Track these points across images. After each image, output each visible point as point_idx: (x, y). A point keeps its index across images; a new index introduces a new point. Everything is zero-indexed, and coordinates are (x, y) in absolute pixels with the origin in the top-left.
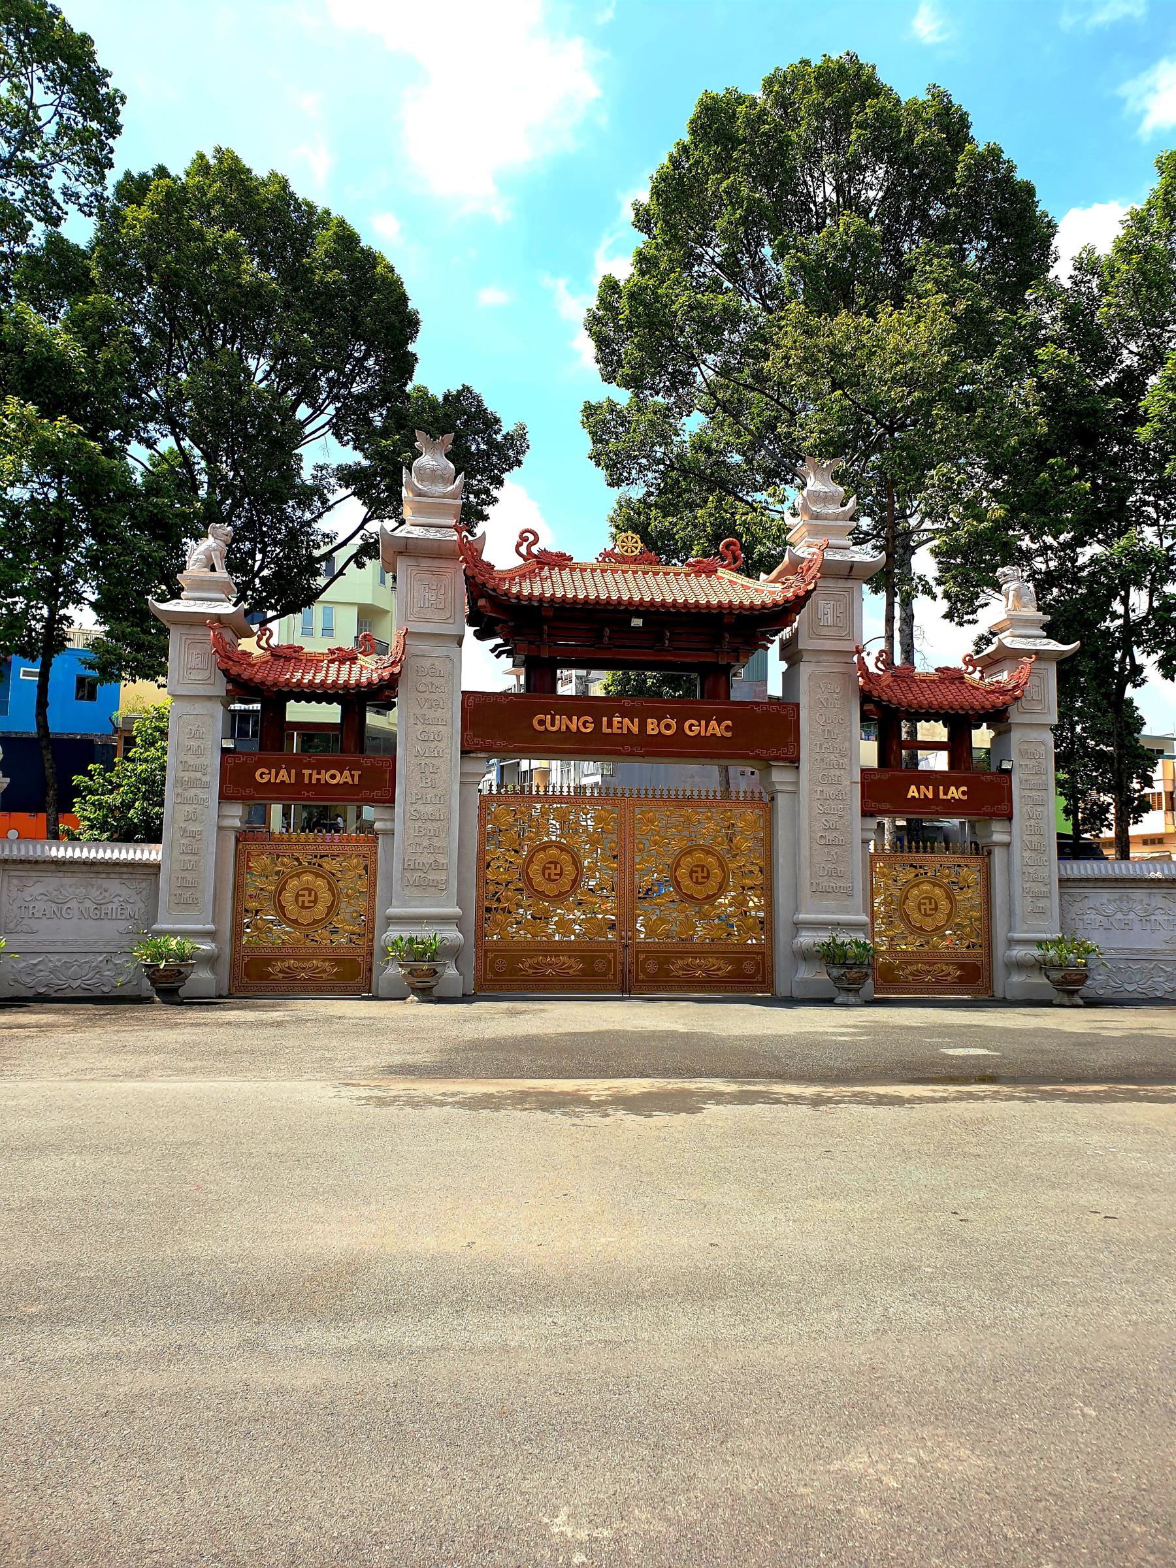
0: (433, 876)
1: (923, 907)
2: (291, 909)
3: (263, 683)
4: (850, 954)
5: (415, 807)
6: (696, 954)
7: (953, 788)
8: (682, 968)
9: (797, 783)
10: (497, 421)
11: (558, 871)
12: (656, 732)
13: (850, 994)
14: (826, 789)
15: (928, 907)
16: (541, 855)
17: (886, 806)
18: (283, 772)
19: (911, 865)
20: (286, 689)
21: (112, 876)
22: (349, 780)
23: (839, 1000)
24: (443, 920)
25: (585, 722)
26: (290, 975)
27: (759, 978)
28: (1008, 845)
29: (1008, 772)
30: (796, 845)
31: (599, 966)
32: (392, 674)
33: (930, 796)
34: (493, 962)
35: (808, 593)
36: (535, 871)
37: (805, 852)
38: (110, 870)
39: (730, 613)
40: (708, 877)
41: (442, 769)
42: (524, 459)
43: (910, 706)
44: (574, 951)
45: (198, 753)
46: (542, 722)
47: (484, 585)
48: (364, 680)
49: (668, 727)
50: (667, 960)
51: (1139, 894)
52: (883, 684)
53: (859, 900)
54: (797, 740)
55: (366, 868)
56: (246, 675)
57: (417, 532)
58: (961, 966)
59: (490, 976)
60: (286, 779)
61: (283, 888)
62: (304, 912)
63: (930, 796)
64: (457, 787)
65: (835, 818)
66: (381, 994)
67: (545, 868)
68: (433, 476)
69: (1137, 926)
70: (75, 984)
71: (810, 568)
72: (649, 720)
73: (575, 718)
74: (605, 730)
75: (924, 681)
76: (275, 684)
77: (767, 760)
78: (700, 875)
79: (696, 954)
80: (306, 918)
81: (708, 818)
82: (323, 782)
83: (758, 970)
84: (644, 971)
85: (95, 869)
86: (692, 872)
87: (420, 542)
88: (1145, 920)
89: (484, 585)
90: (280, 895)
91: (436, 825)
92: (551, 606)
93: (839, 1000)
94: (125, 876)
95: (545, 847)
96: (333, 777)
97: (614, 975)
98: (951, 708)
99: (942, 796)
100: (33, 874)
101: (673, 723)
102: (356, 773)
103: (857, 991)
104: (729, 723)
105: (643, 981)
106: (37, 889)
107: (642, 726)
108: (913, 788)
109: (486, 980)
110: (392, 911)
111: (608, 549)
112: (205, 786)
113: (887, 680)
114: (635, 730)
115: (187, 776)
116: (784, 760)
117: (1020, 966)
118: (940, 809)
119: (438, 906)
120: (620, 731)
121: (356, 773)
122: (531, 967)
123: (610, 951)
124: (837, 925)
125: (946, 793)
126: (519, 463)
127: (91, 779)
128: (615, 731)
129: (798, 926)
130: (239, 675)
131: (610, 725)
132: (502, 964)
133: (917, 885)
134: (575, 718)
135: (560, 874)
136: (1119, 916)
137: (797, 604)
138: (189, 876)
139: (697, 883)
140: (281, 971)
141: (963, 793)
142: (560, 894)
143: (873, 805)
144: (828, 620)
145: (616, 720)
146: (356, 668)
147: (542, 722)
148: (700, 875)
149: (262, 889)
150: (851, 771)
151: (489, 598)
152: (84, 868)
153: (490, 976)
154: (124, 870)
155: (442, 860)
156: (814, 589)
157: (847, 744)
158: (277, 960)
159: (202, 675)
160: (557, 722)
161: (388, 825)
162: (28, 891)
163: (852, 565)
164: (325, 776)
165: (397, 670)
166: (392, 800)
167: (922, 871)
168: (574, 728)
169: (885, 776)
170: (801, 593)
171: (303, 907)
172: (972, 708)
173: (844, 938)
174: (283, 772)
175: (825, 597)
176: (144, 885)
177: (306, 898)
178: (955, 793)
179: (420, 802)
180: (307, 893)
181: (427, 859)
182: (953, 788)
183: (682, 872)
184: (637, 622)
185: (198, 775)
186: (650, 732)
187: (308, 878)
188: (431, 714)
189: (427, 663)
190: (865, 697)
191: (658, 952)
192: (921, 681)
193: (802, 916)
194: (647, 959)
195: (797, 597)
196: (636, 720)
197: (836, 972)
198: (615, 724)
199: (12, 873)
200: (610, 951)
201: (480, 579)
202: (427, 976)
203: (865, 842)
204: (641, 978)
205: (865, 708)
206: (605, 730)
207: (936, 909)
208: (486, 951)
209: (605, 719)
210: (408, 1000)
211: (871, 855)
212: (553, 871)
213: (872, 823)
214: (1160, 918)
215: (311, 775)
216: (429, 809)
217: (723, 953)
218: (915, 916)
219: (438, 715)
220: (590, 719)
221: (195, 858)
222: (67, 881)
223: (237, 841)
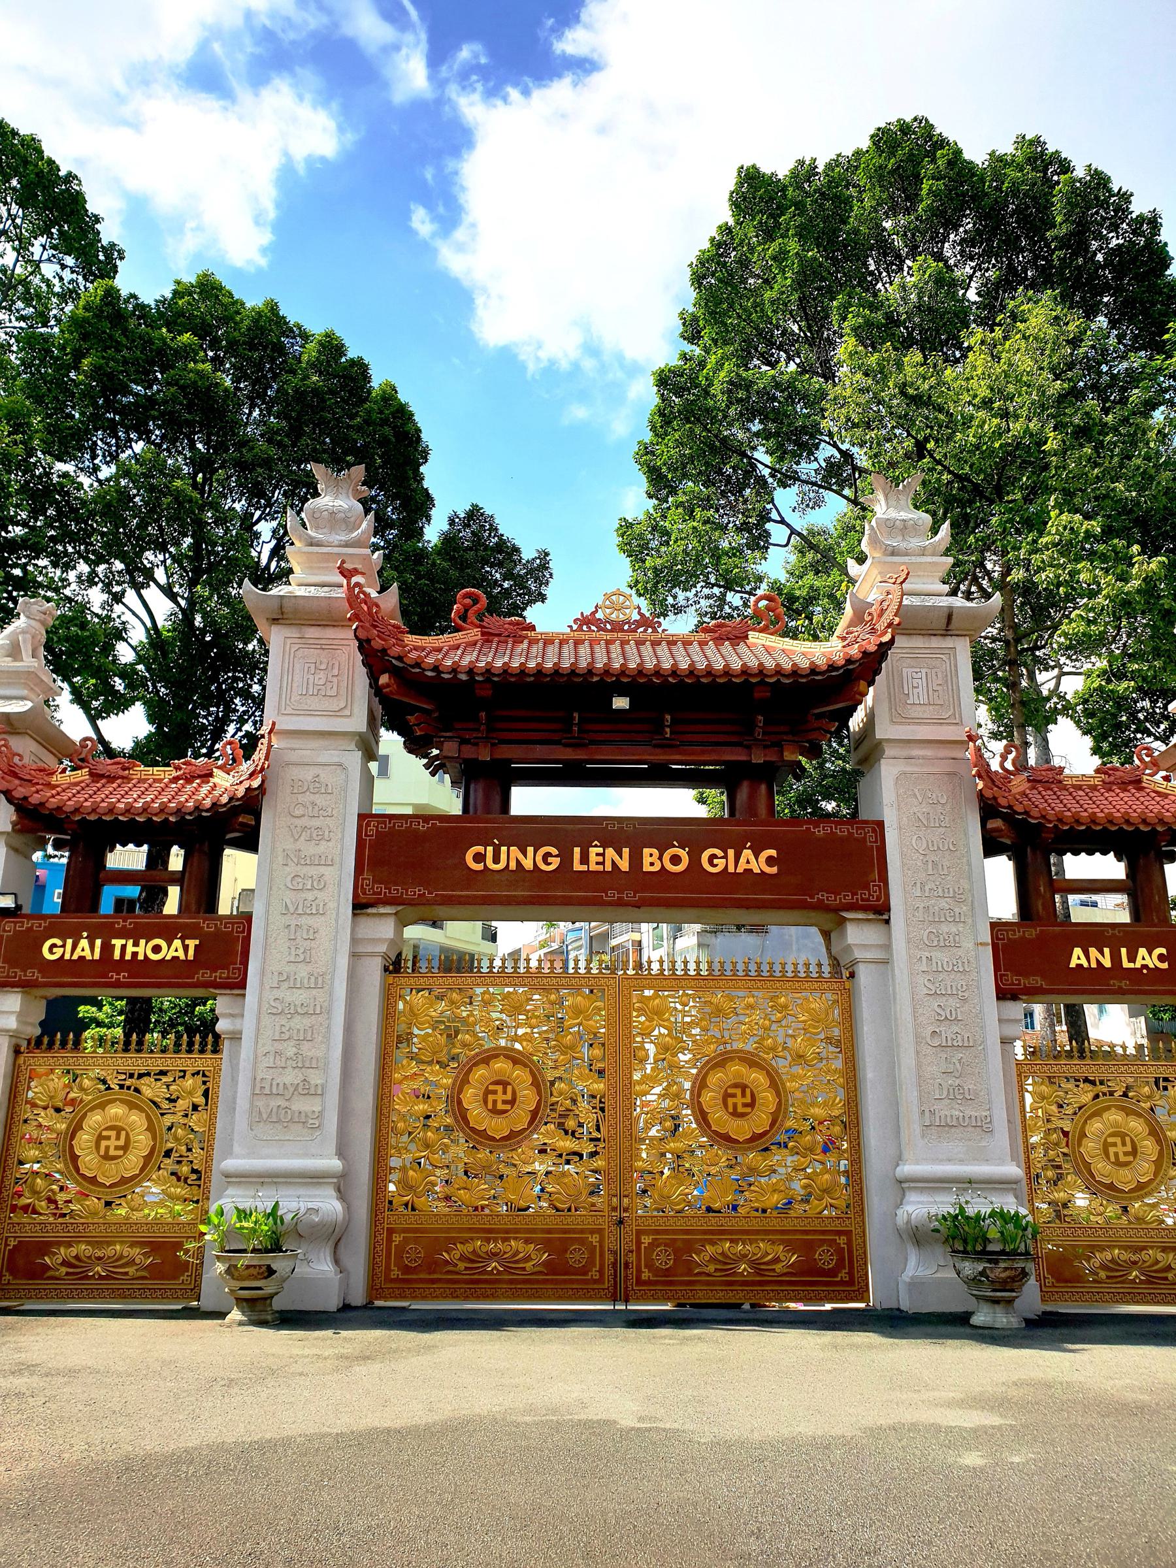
0: (301, 1105)
1: (1112, 1150)
2: (89, 1161)
3: (59, 809)
4: (993, 1233)
6: (735, 1235)
7: (1142, 951)
8: (713, 1259)
9: (888, 947)
10: (516, 550)
11: (509, 1097)
12: (656, 868)
13: (998, 1308)
14: (937, 955)
15: (1120, 1149)
16: (480, 1072)
17: (1037, 981)
18: (84, 943)
19: (1086, 1080)
20: (92, 817)
22: (181, 954)
23: (977, 1320)
24: (313, 1178)
26: (78, 1269)
27: (843, 1275)
30: (891, 1049)
31: (576, 1257)
32: (248, 790)
33: (1107, 963)
34: (400, 1249)
35: (884, 649)
36: (470, 1097)
39: (762, 683)
40: (752, 1105)
42: (548, 591)
43: (1060, 820)
44: (533, 1231)
46: (479, 858)
47: (384, 651)
48: (208, 803)
49: (675, 860)
50: (689, 1247)
52: (1014, 791)
53: (1001, 1139)
55: (206, 1094)
56: (35, 799)
57: (301, 592)
59: (395, 1273)
60: (87, 954)
61: (78, 1127)
62: (110, 1166)
63: (1107, 963)
64: (343, 962)
65: (953, 1002)
66: (206, 1303)
67: (487, 1092)
68: (334, 520)
71: (882, 612)
72: (646, 851)
73: (530, 850)
74: (578, 866)
75: (1080, 788)
76: (77, 810)
77: (836, 910)
78: (739, 1100)
79: (735, 1235)
80: (109, 1174)
81: (750, 1007)
82: (141, 957)
83: (841, 1260)
84: (649, 1266)
86: (727, 1096)
87: (301, 602)
89: (384, 651)
90: (72, 1138)
91: (307, 1021)
93: (977, 1320)
95: (487, 1058)
96: (156, 949)
97: (601, 1271)
98: (1127, 822)
99: (1126, 964)
101: (683, 854)
102: (192, 943)
103: (1010, 1302)
104: (773, 852)
105: (649, 1282)
107: (636, 860)
108: (1078, 951)
109: (389, 1280)
110: (231, 1164)
111: (587, 613)
113: (1019, 784)
114: (624, 865)
116: (865, 909)
119: (306, 1155)
120: (600, 868)
121: (192, 943)
122: (463, 1258)
123: (592, 1232)
124: (969, 1183)
125: (1132, 959)
126: (542, 598)
127: (100, 1009)
128: (593, 867)
129: (904, 1185)
130: (42, 804)
131: (585, 859)
132: (415, 1254)
133: (1097, 1114)
134: (530, 850)
135: (512, 1102)
137: (868, 666)
139: (735, 1114)
140: (65, 1263)
141: (1161, 958)
142: (512, 1135)
143: (1012, 978)
144: (919, 695)
145: (593, 851)
146: (205, 789)
147: (479, 858)
148: (739, 1100)
149: (49, 1128)
150: (974, 925)
151: (395, 672)
153: (395, 1273)
155: (316, 1079)
156: (892, 641)
157: (965, 884)
158: (59, 1244)
160: (503, 857)
163: (950, 615)
164: (144, 949)
165: (256, 783)
166: (242, 985)
167: (1104, 1089)
168: (528, 864)
169: (1032, 933)
170: (872, 648)
171: (107, 1157)
172: (1161, 821)
173: (979, 1206)
174: (84, 943)
175: (913, 662)
177: (113, 1143)
178: (1148, 958)
179: (286, 985)
180: (113, 1133)
181: (291, 1077)
182: (1142, 951)
183: (708, 1098)
184: (621, 703)
186: (647, 868)
187: (116, 1110)
188: (310, 849)
189: (308, 774)
190: (988, 809)
191: (675, 1232)
192: (1073, 786)
193: (907, 1169)
195: (865, 654)
196: (626, 851)
197: (970, 1268)
198: (593, 858)
200: (592, 1232)
201: (378, 643)
202: (256, 1278)
203: (1007, 1042)
204: (646, 1275)
205: (991, 824)
206: (578, 866)
207: (1134, 1152)
208: (391, 1231)
209: (577, 850)
211: (1019, 1064)
212: (500, 1097)
213: (1016, 1009)
215: (124, 947)
216: (299, 997)
217: (783, 1232)
218: (1101, 1167)
220: (554, 851)
223: (17, 1051)
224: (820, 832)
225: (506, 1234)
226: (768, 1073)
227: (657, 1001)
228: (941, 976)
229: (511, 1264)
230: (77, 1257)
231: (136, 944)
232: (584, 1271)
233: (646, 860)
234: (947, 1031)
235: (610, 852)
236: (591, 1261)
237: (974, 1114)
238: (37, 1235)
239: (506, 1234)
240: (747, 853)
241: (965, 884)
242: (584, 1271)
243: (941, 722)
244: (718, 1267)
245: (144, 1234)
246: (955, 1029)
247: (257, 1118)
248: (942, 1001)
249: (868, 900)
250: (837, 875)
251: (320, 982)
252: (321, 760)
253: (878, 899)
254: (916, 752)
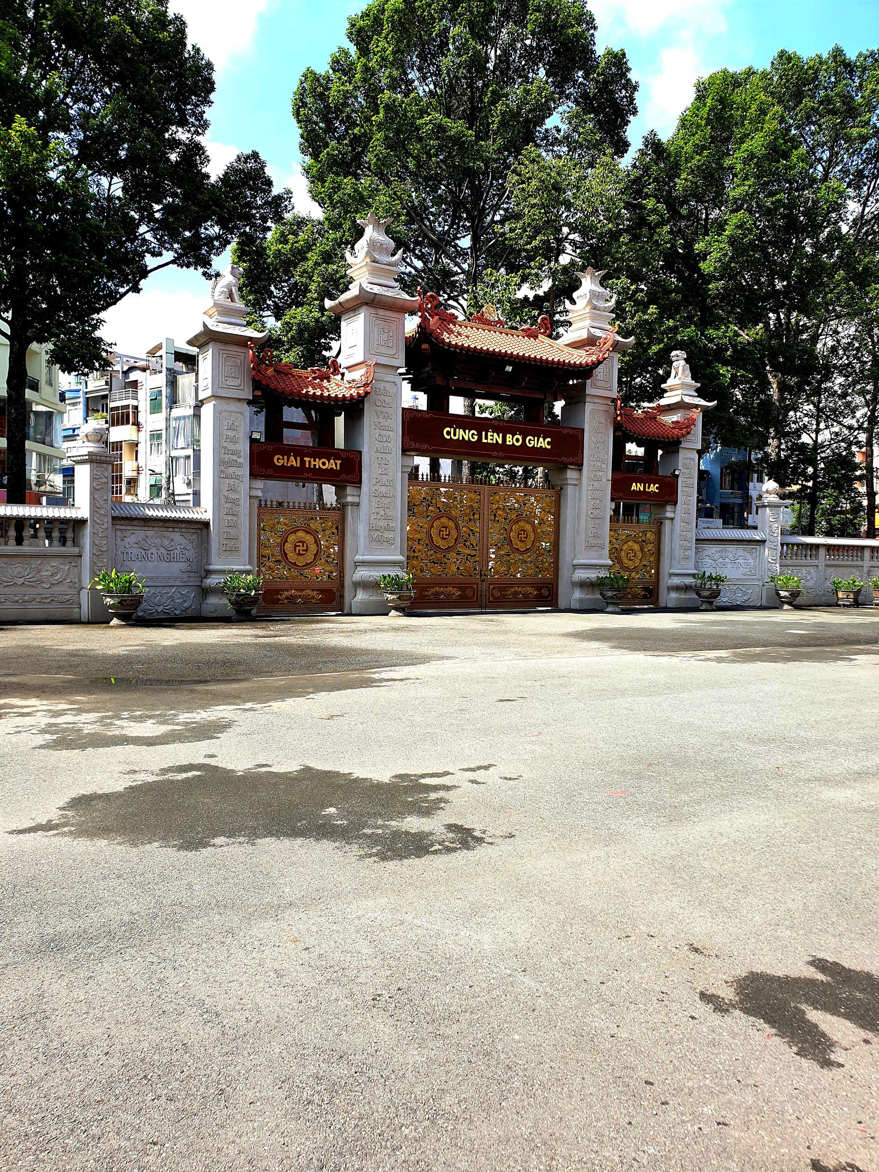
2: (292, 557)
3: (283, 393)
5: (375, 487)
9: (580, 479)
14: (595, 484)
18: (292, 458)
24: (393, 563)
25: (473, 434)
28: (672, 519)
29: (678, 476)
31: (469, 593)
37: (583, 522)
38: (175, 525)
41: (391, 462)
45: (234, 441)
46: (448, 433)
49: (518, 440)
50: (505, 589)
51: (731, 548)
55: (337, 528)
58: (645, 589)
64: (400, 475)
65: (598, 502)
69: (729, 566)
70: (160, 609)
71: (605, 343)
72: (508, 435)
74: (484, 441)
76: (291, 394)
85: (167, 525)
87: (383, 298)
88: (733, 562)
91: (388, 500)
92: (467, 353)
94: (183, 530)
96: (324, 464)
100: (129, 528)
102: (339, 462)
104: (549, 439)
106: (132, 539)
107: (504, 439)
110: (358, 558)
112: (240, 466)
114: (500, 441)
115: (227, 457)
117: (677, 588)
118: (645, 497)
121: (339, 462)
128: (490, 441)
129: (575, 567)
131: (486, 438)
136: (721, 560)
138: (232, 531)
140: (287, 598)
143: (616, 495)
145: (489, 434)
147: (448, 433)
151: (431, 343)
152: (161, 524)
154: (184, 525)
159: (236, 382)
161: (356, 499)
162: (127, 540)
164: (318, 463)
166: (360, 482)
168: (466, 438)
172: (668, 438)
176: (194, 536)
178: (653, 488)
181: (383, 523)
184: (509, 369)
185: (235, 458)
186: (508, 443)
189: (382, 385)
194: (494, 588)
198: (490, 437)
199: (118, 527)
204: (491, 599)
206: (484, 441)
209: (484, 433)
210: (112, 623)
214: (741, 561)
216: (383, 489)
219: (387, 423)
221: (235, 518)
222: (149, 533)
224: (565, 432)
225: (446, 585)
229: (450, 595)
230: (291, 595)
231: (315, 461)
233: (508, 440)
235: (495, 434)
236: (474, 595)
238: (279, 587)
239: (446, 585)
240: (541, 439)
243: (606, 389)
245: (318, 587)
247: (372, 540)
250: (567, 450)
251: (391, 483)
252: (386, 379)
254: (596, 401)
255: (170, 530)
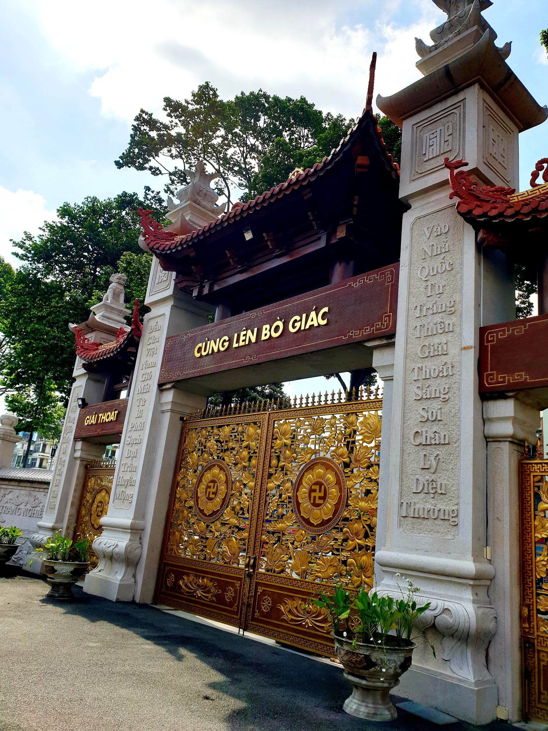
21: (41, 490)
38: (39, 486)
53: (466, 533)
54: (394, 309)
65: (436, 405)
100: (10, 487)
116: (380, 338)
194: (264, 593)
222: (23, 492)
226: (336, 473)
227: (285, 426)
228: (429, 382)
232: (231, 604)
234: (429, 430)
237: (443, 507)
241: (457, 298)
242: (231, 604)
244: (293, 618)
246: (435, 428)
248: (426, 404)
249: (380, 329)
253: (388, 325)
255: (37, 490)
